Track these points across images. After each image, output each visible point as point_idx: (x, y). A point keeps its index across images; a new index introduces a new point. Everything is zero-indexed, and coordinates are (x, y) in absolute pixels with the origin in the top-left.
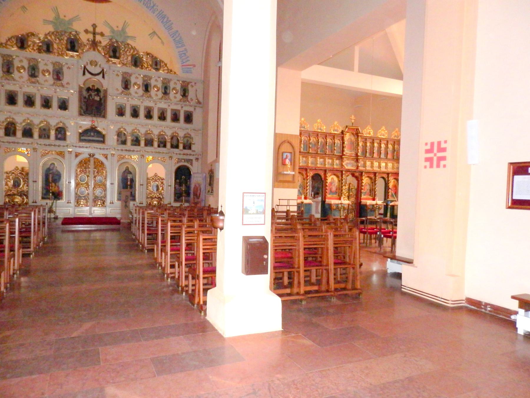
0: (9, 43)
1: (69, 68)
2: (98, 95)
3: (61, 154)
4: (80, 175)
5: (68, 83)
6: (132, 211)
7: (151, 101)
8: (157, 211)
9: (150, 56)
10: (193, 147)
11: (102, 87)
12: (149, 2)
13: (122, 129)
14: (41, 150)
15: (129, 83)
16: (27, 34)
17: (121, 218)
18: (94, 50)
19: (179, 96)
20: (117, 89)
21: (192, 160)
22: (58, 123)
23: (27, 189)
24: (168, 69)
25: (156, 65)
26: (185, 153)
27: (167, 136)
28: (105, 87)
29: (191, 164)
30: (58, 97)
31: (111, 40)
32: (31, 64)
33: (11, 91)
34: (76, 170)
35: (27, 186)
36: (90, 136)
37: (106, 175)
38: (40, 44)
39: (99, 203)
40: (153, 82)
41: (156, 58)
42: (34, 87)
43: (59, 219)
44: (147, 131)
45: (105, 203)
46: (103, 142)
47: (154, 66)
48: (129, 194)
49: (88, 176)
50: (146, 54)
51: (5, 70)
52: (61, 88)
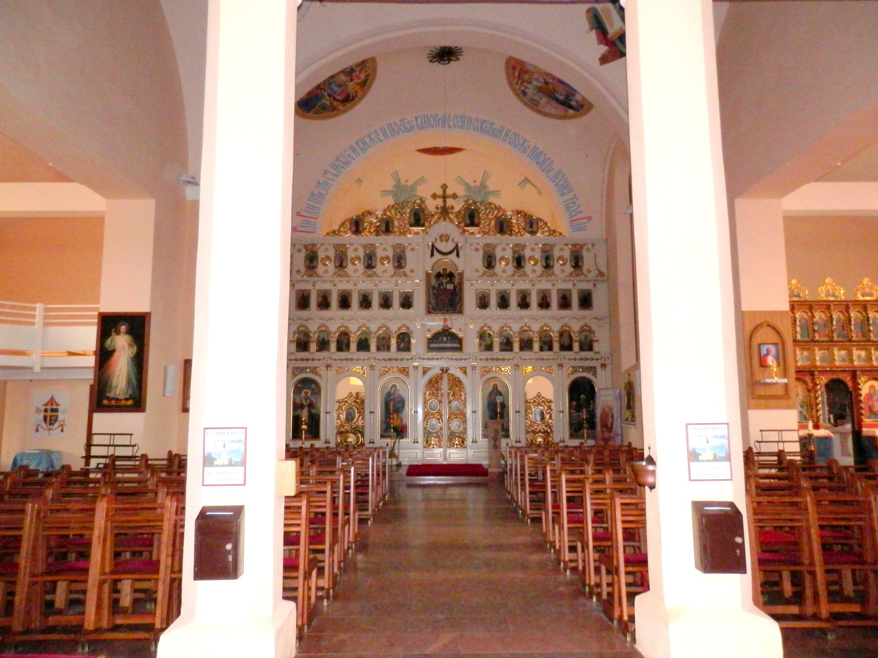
0: (342, 229)
1: (413, 249)
2: (451, 282)
3: (404, 371)
4: (430, 401)
5: (412, 271)
6: (504, 453)
7: (526, 281)
8: (543, 455)
9: (521, 215)
10: (596, 347)
11: (457, 270)
12: (517, 139)
13: (485, 328)
15: (493, 259)
16: (363, 214)
17: (489, 466)
18: (445, 220)
19: (569, 268)
20: (477, 270)
21: (595, 368)
22: (400, 328)
23: (362, 423)
24: (550, 230)
25: (531, 226)
26: (583, 357)
27: (553, 333)
28: (460, 270)
29: (595, 374)
30: (400, 292)
31: (466, 201)
32: (367, 252)
33: (343, 291)
34: (425, 394)
35: (363, 419)
36: (442, 342)
37: (465, 398)
38: (378, 224)
39: (457, 442)
40: (527, 253)
41: (531, 216)
42: (370, 281)
43: (403, 467)
44: (522, 327)
45: (465, 442)
46: (460, 349)
47: (528, 229)
48: (499, 427)
49: (440, 402)
50: (516, 214)
51: (337, 264)
52: (404, 278)
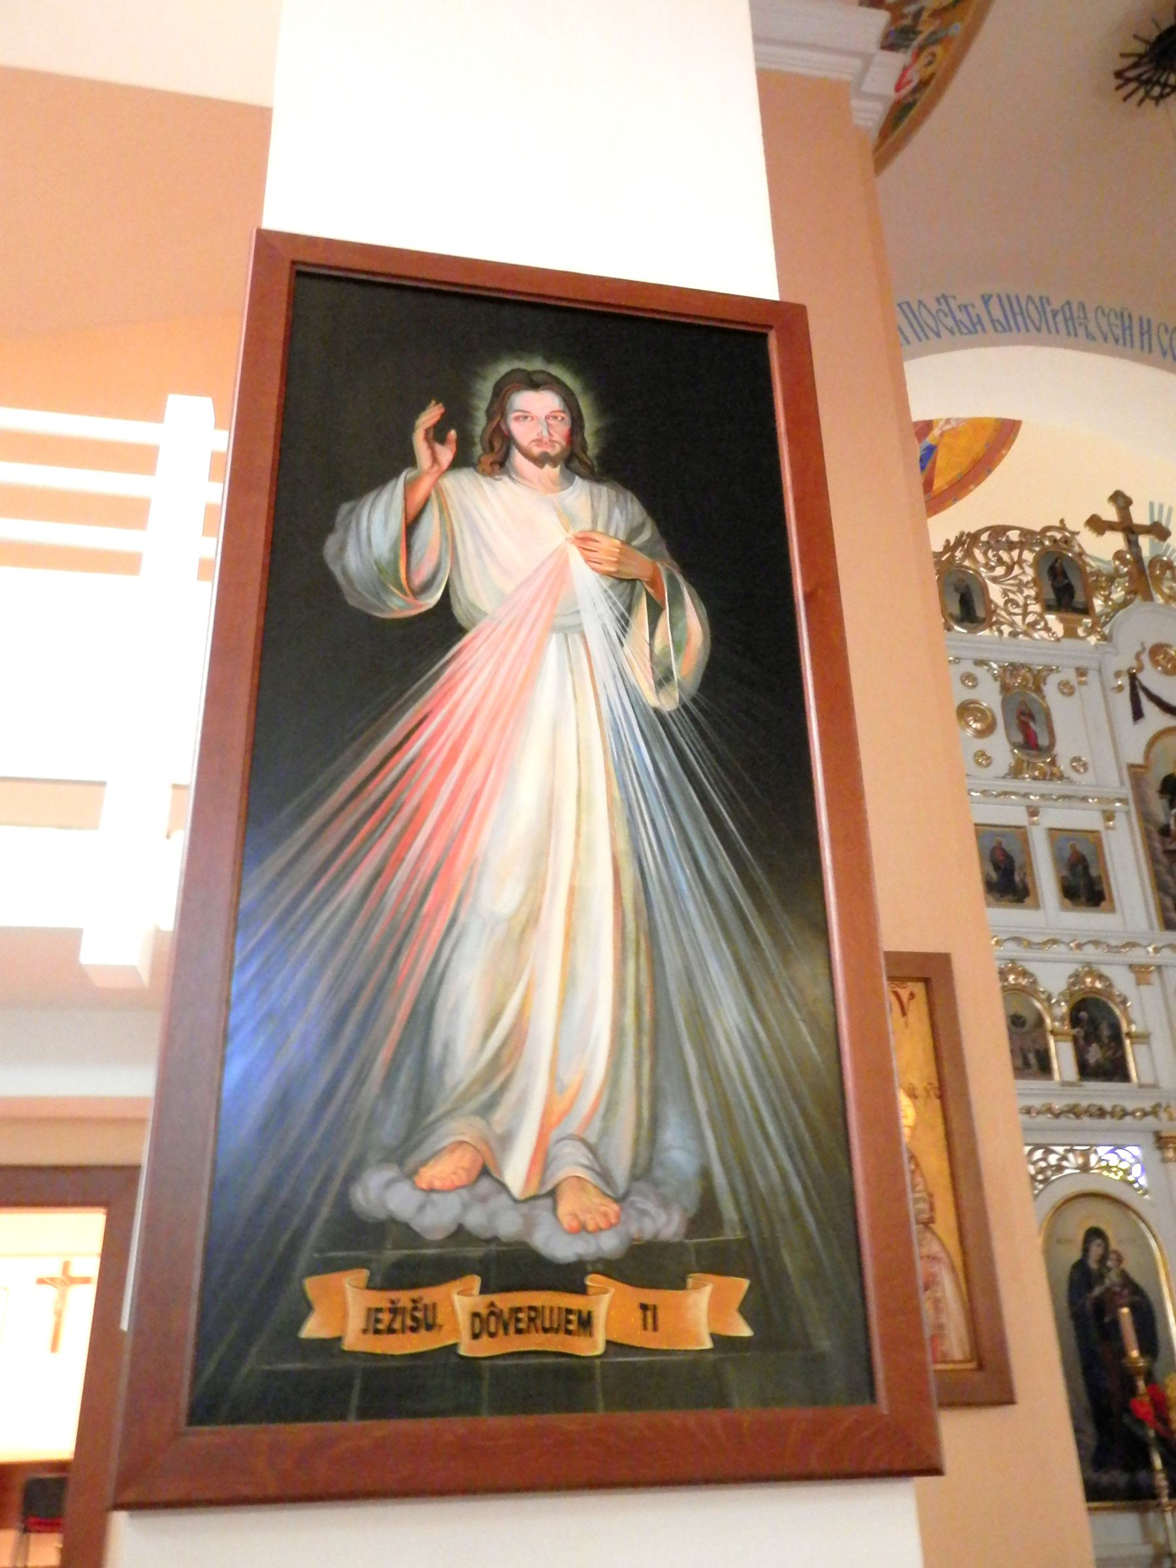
14: (1028, 1149)
